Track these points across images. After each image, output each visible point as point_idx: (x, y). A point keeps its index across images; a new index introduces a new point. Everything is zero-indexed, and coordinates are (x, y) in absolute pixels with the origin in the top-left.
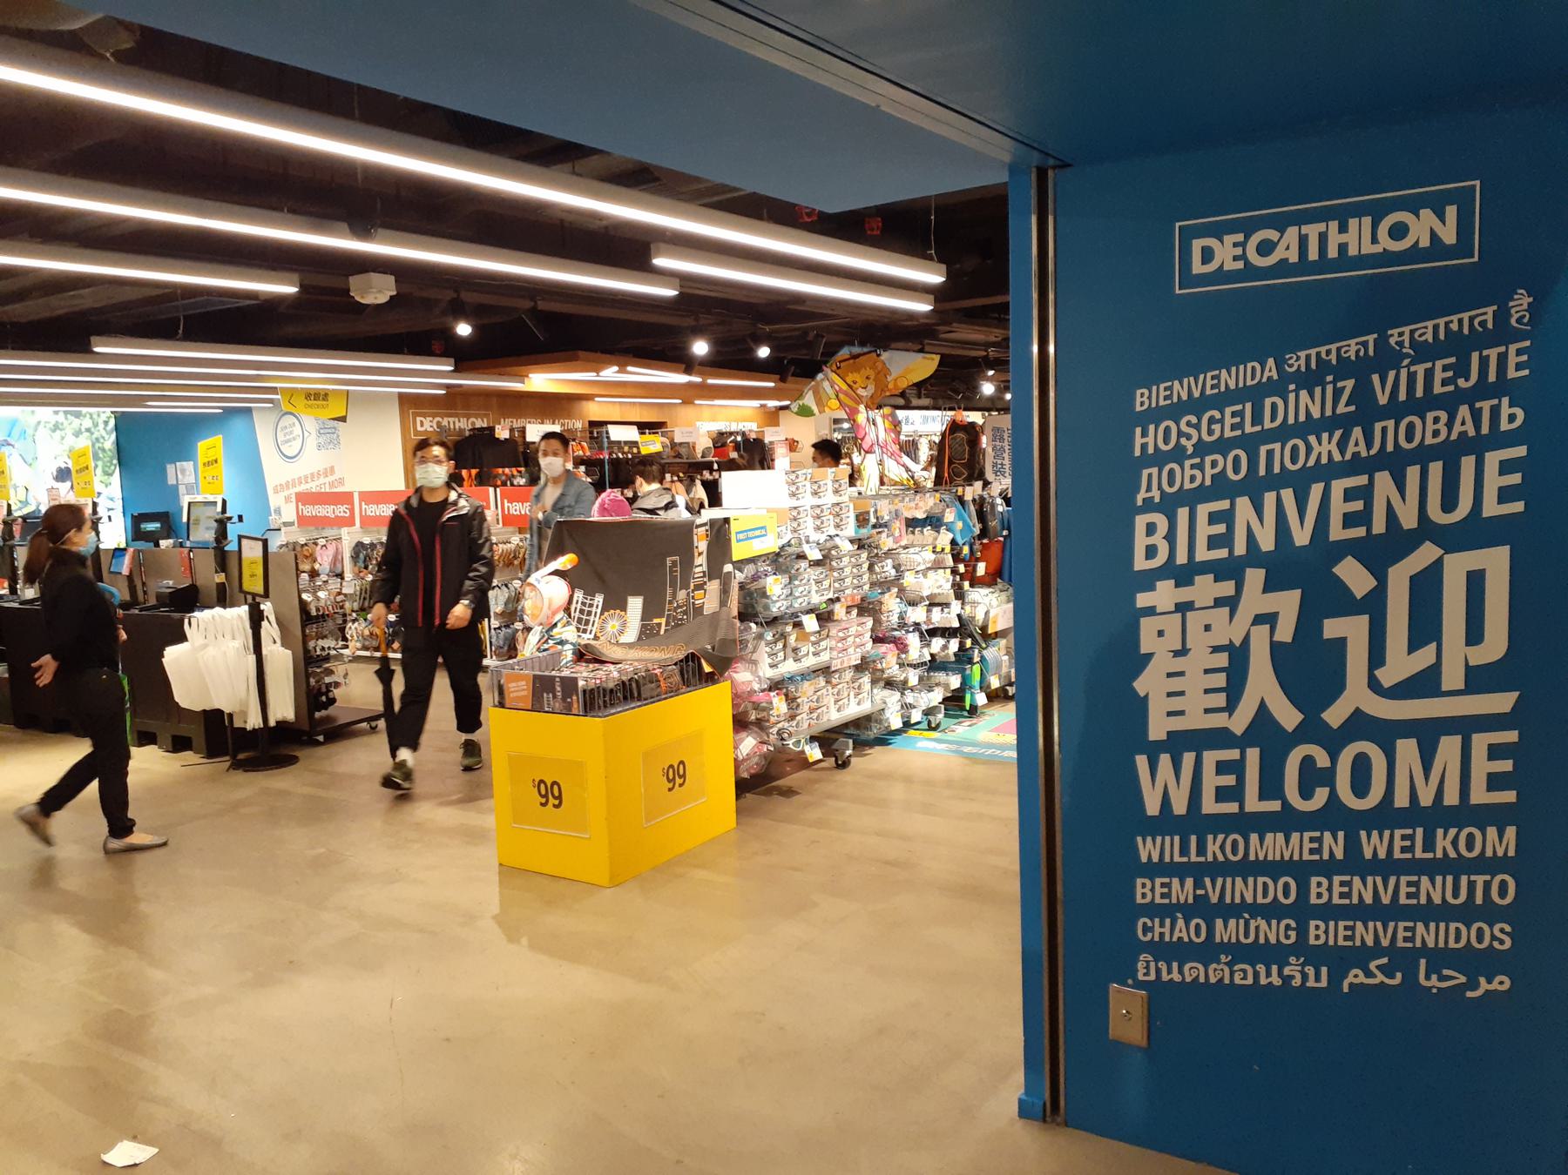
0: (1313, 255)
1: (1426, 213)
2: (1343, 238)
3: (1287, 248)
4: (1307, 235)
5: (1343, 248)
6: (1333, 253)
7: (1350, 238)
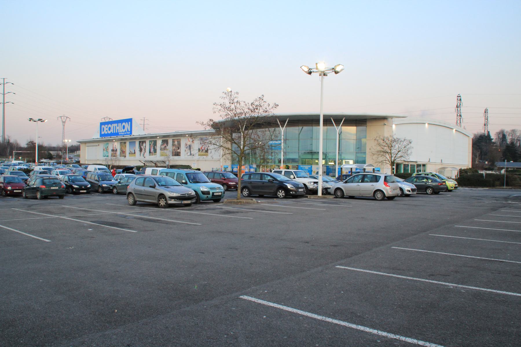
0: (115, 132)
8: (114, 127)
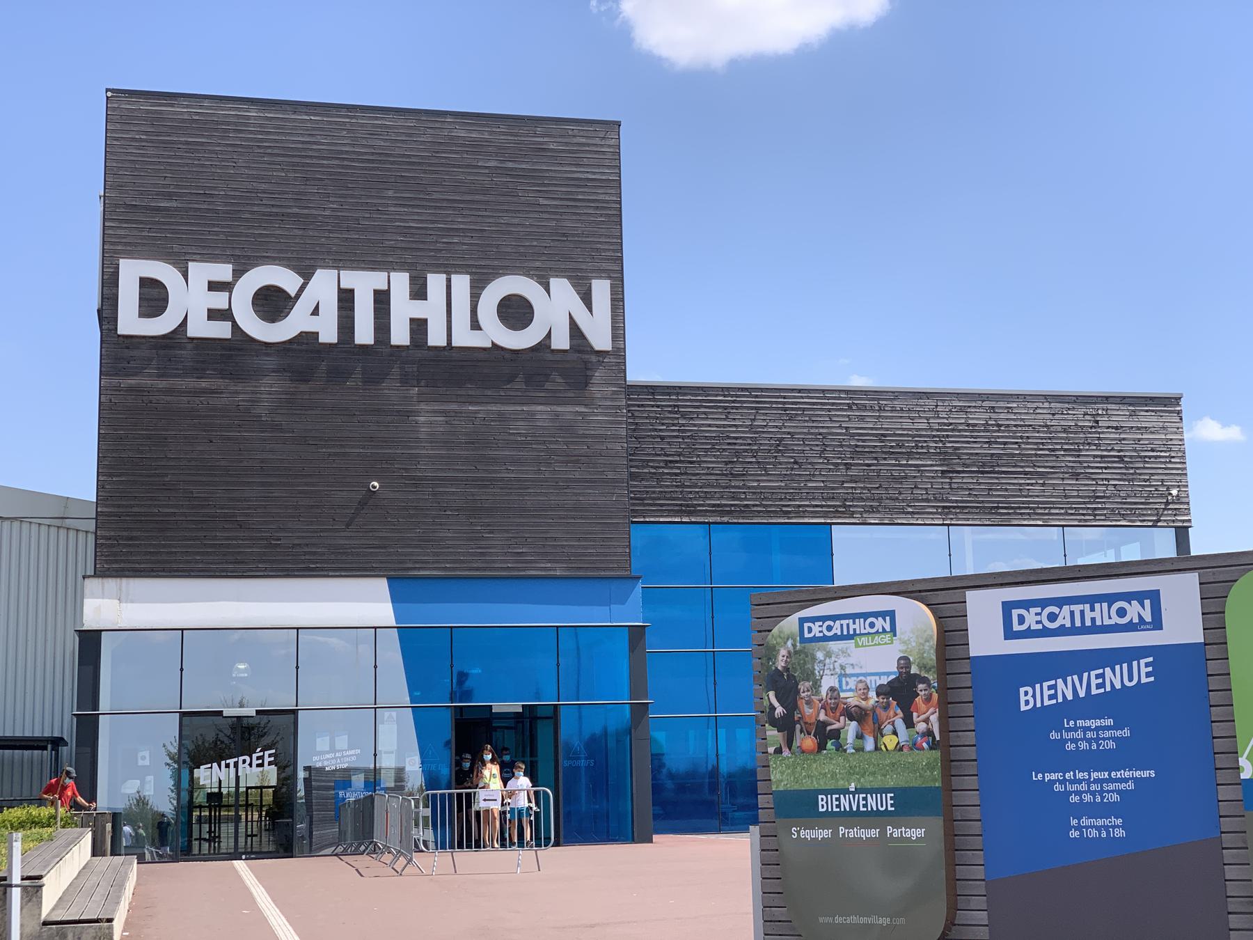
0: (1078, 624)
1: (1134, 603)
2: (1093, 615)
3: (1064, 618)
4: (1073, 611)
5: (1093, 620)
6: (1088, 623)
7: (1097, 614)
8: (1072, 613)
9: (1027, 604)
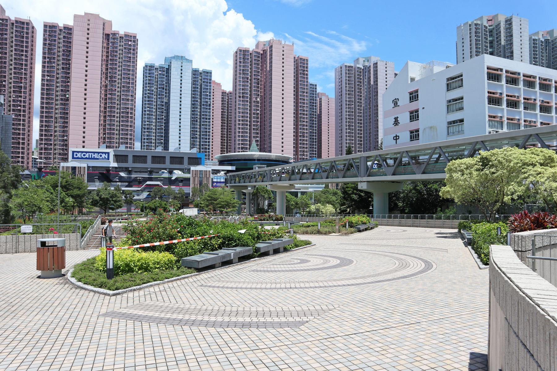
0: (90, 157)
6: (93, 157)
7: (95, 156)
9: (78, 152)
